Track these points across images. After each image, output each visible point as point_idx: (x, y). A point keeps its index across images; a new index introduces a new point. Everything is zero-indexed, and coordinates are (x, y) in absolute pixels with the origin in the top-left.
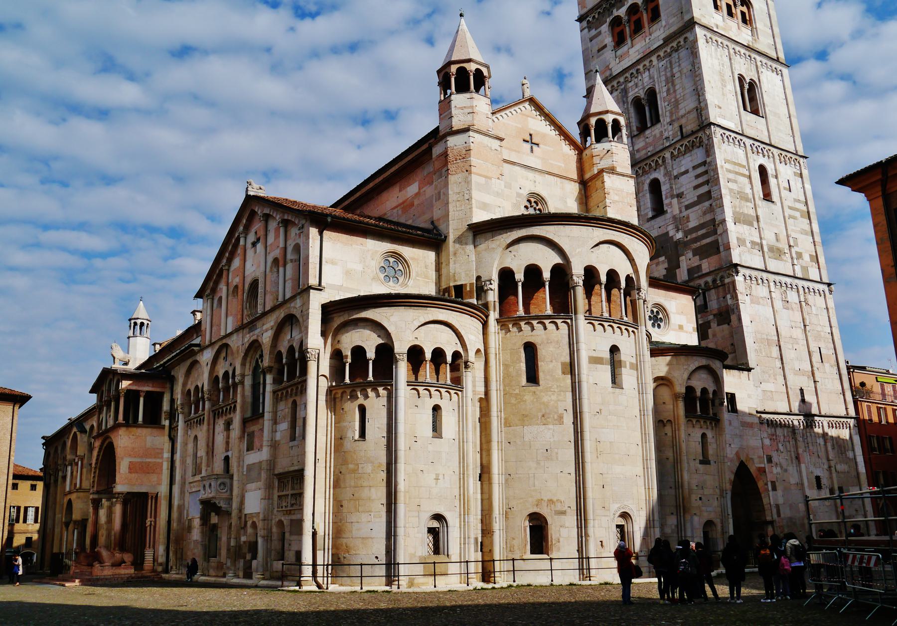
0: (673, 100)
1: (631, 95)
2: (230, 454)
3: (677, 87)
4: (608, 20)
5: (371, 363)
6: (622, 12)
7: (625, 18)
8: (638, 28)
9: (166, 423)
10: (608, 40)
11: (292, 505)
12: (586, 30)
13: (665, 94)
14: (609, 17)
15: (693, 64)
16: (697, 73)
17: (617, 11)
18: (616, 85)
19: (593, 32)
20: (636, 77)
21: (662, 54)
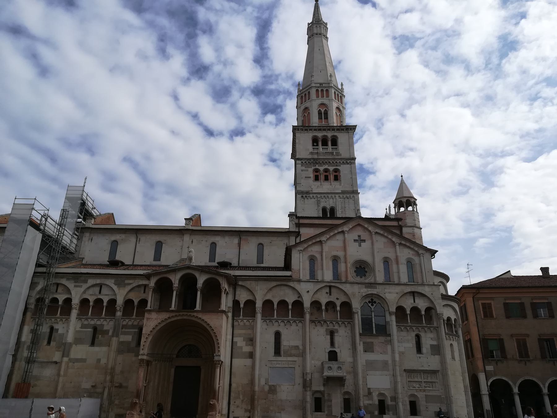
1: (322, 205)
2: (337, 350)
3: (346, 213)
4: (313, 167)
5: (453, 325)
6: (321, 168)
8: (327, 178)
9: (230, 315)
10: (312, 175)
11: (425, 387)
12: (300, 165)
13: (340, 213)
14: (314, 166)
18: (315, 197)
19: (303, 168)
20: (326, 199)
21: (341, 196)
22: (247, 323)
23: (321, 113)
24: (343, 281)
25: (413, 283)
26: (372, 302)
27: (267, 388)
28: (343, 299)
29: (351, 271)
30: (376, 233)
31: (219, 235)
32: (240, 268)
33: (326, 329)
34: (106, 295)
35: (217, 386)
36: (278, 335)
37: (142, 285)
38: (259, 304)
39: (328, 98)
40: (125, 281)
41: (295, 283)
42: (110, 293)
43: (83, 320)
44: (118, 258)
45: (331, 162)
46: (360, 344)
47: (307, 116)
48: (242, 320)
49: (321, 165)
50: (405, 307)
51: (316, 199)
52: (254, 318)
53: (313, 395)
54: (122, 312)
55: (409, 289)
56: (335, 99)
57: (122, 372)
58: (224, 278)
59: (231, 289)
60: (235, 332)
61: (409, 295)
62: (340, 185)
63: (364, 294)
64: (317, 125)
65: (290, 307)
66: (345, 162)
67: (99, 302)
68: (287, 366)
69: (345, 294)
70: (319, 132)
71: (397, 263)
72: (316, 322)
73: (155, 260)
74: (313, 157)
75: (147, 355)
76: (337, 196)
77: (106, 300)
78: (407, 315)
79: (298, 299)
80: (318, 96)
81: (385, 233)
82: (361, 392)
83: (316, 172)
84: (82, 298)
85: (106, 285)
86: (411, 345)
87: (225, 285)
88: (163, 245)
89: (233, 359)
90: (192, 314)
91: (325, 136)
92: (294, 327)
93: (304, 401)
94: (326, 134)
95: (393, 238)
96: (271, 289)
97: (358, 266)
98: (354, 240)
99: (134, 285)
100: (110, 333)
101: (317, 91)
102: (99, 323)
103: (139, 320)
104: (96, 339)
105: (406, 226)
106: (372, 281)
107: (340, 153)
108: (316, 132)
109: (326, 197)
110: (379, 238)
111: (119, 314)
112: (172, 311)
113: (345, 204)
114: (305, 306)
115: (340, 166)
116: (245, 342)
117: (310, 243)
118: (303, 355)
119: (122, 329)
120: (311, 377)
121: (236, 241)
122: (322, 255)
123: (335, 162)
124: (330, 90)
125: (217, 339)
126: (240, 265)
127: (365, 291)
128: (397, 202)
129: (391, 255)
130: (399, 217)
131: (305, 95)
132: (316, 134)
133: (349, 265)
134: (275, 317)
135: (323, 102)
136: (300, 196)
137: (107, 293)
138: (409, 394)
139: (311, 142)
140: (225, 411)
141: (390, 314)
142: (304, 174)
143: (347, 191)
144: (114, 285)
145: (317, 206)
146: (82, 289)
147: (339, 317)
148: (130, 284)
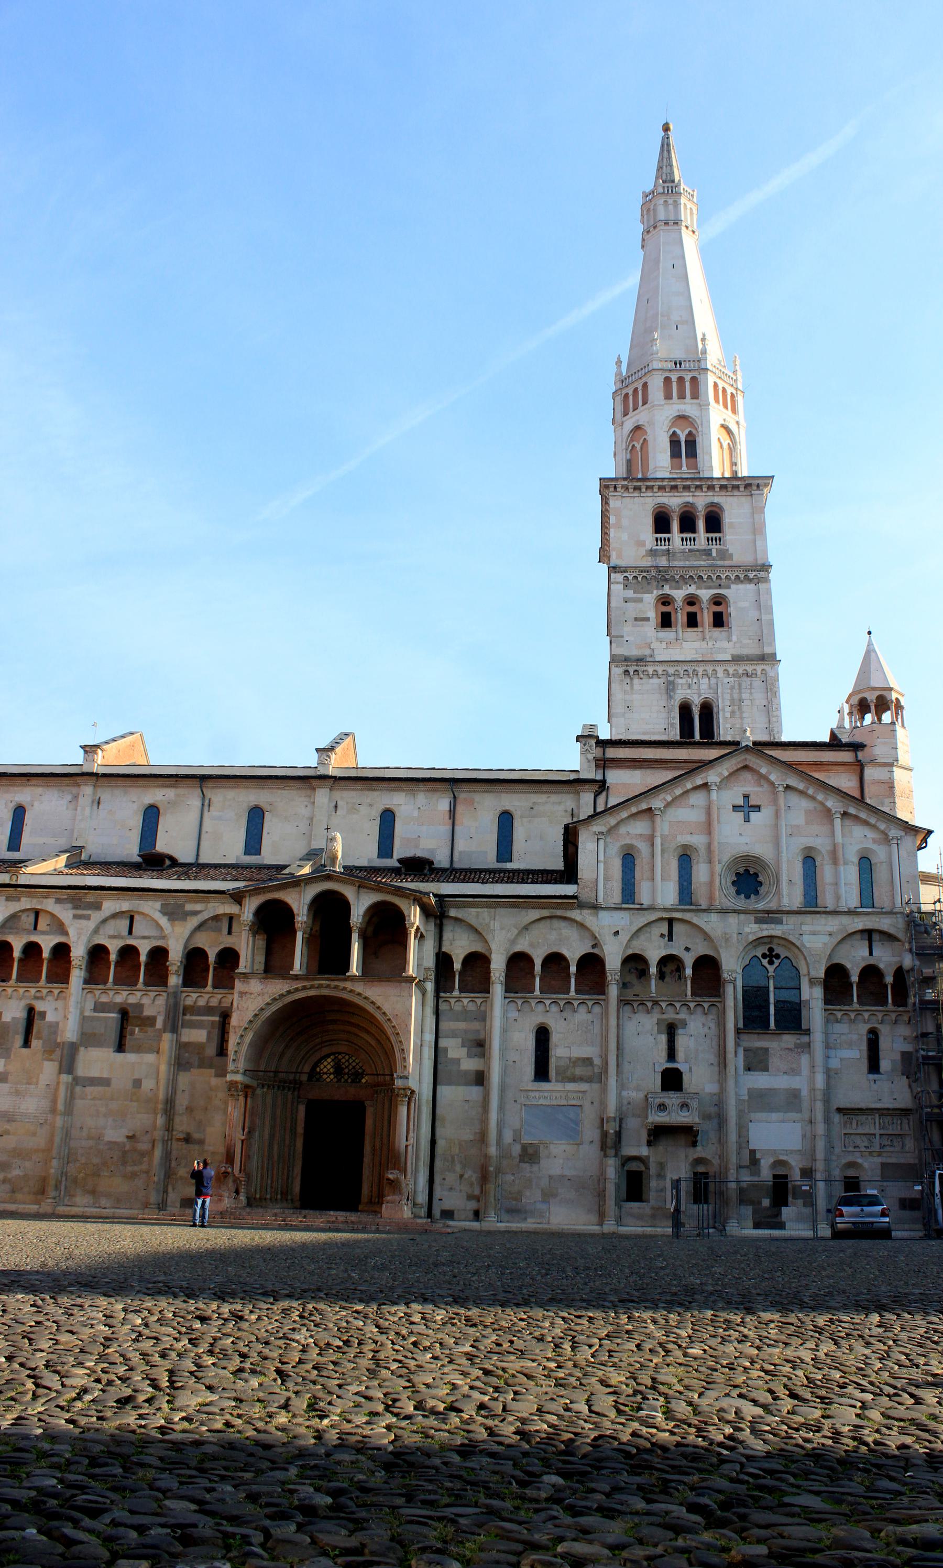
0: (738, 726)
1: (681, 694)
2: (681, 1066)
3: (744, 715)
4: (655, 592)
6: (679, 595)
7: (679, 603)
8: (692, 621)
9: (430, 986)
10: (652, 614)
12: (622, 586)
13: (728, 715)
14: (657, 588)
15: (770, 702)
16: (775, 713)
17: (670, 588)
18: (660, 672)
19: (630, 593)
22: (471, 1007)
23: (679, 442)
24: (703, 907)
25: (870, 910)
26: (771, 956)
27: (517, 1150)
28: (701, 949)
29: (723, 881)
30: (788, 787)
31: (401, 790)
32: (454, 873)
33: (658, 1019)
34: (144, 937)
35: (404, 1143)
36: (542, 1035)
37: (224, 915)
38: (498, 965)
39: (695, 401)
40: (183, 906)
41: (586, 912)
42: (153, 932)
43: (97, 993)
44: (161, 846)
45: (705, 577)
46: (736, 1052)
47: (641, 448)
48: (459, 1000)
49: (677, 583)
50: (849, 966)
51: (662, 680)
52: (487, 995)
53: (623, 1165)
54: (181, 978)
55: (860, 924)
56: (717, 401)
57: (190, 1110)
58: (412, 902)
59: (432, 927)
60: (444, 1026)
61: (858, 936)
62: (729, 640)
63: (752, 938)
64: (667, 475)
65: (573, 969)
66: (742, 576)
67: (129, 952)
68: (564, 1102)
69: (707, 937)
70: (671, 494)
71: (835, 861)
72: (635, 1005)
73: (247, 852)
74: (655, 564)
75: (245, 1072)
76: (720, 670)
77: (144, 949)
78: (851, 985)
79: (592, 951)
80: (668, 396)
81: (808, 789)
82: (733, 1159)
83: (664, 604)
84: (91, 945)
85: (143, 914)
86: (857, 1053)
87: (415, 916)
88: (267, 816)
89: (439, 1088)
90: (342, 984)
91: (687, 504)
92: (582, 1015)
93: (602, 1177)
94: (690, 500)
95: (826, 799)
96: (526, 928)
97: (741, 870)
98: (734, 807)
99: (206, 915)
100: (159, 1024)
101: (667, 380)
102: (132, 1000)
103: (220, 996)
104: (128, 1037)
105: (873, 762)
106: (773, 906)
107: (730, 552)
108: (665, 494)
109: (691, 672)
110: (794, 799)
111: (174, 980)
112: (296, 978)
113: (740, 693)
114: (608, 967)
115: (729, 587)
116: (465, 1049)
117: (624, 814)
118: (599, 1077)
119: (184, 1014)
120: (620, 1126)
121: (444, 804)
122: (652, 845)
123: (714, 578)
124: (701, 378)
125: (401, 1042)
126: (456, 866)
127: (753, 930)
128: (855, 700)
129: (821, 843)
130: (858, 739)
131: (636, 390)
132: (665, 500)
133: (718, 868)
134: (537, 992)
135: (685, 411)
136: (620, 671)
137: (146, 934)
138: (844, 1161)
139: (649, 523)
140: (422, 1198)
141: (812, 982)
142: (632, 610)
143: (747, 656)
144: (161, 915)
145: (665, 697)
146: (91, 925)
147: (689, 993)
148: (195, 913)
